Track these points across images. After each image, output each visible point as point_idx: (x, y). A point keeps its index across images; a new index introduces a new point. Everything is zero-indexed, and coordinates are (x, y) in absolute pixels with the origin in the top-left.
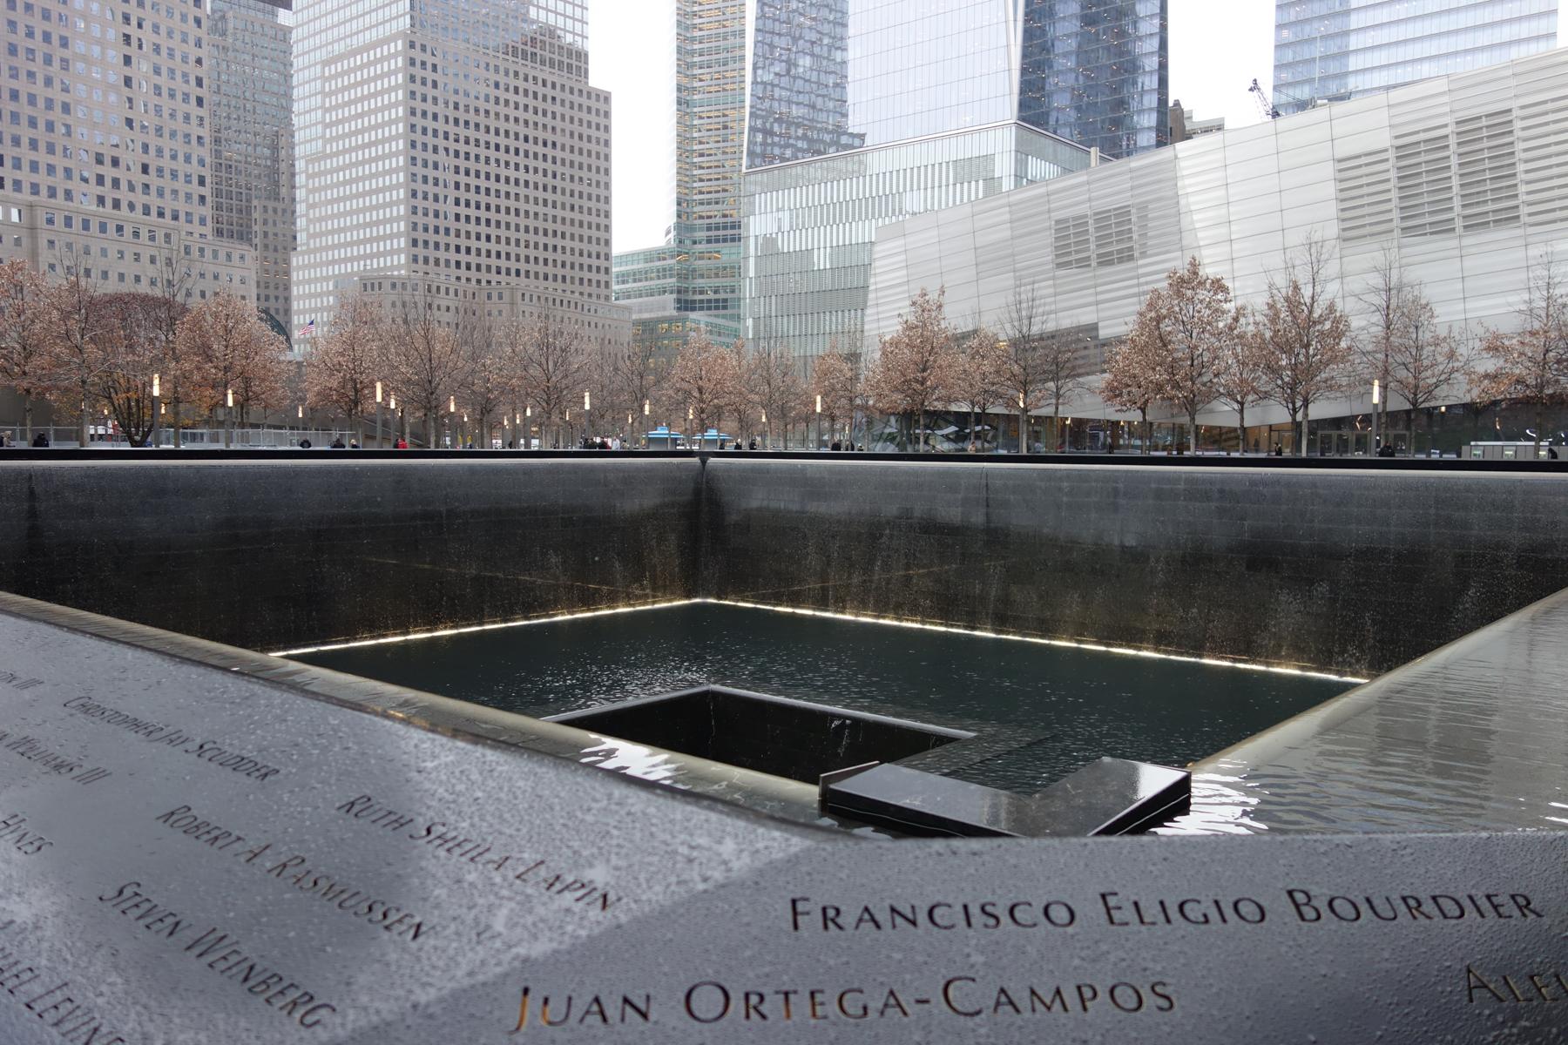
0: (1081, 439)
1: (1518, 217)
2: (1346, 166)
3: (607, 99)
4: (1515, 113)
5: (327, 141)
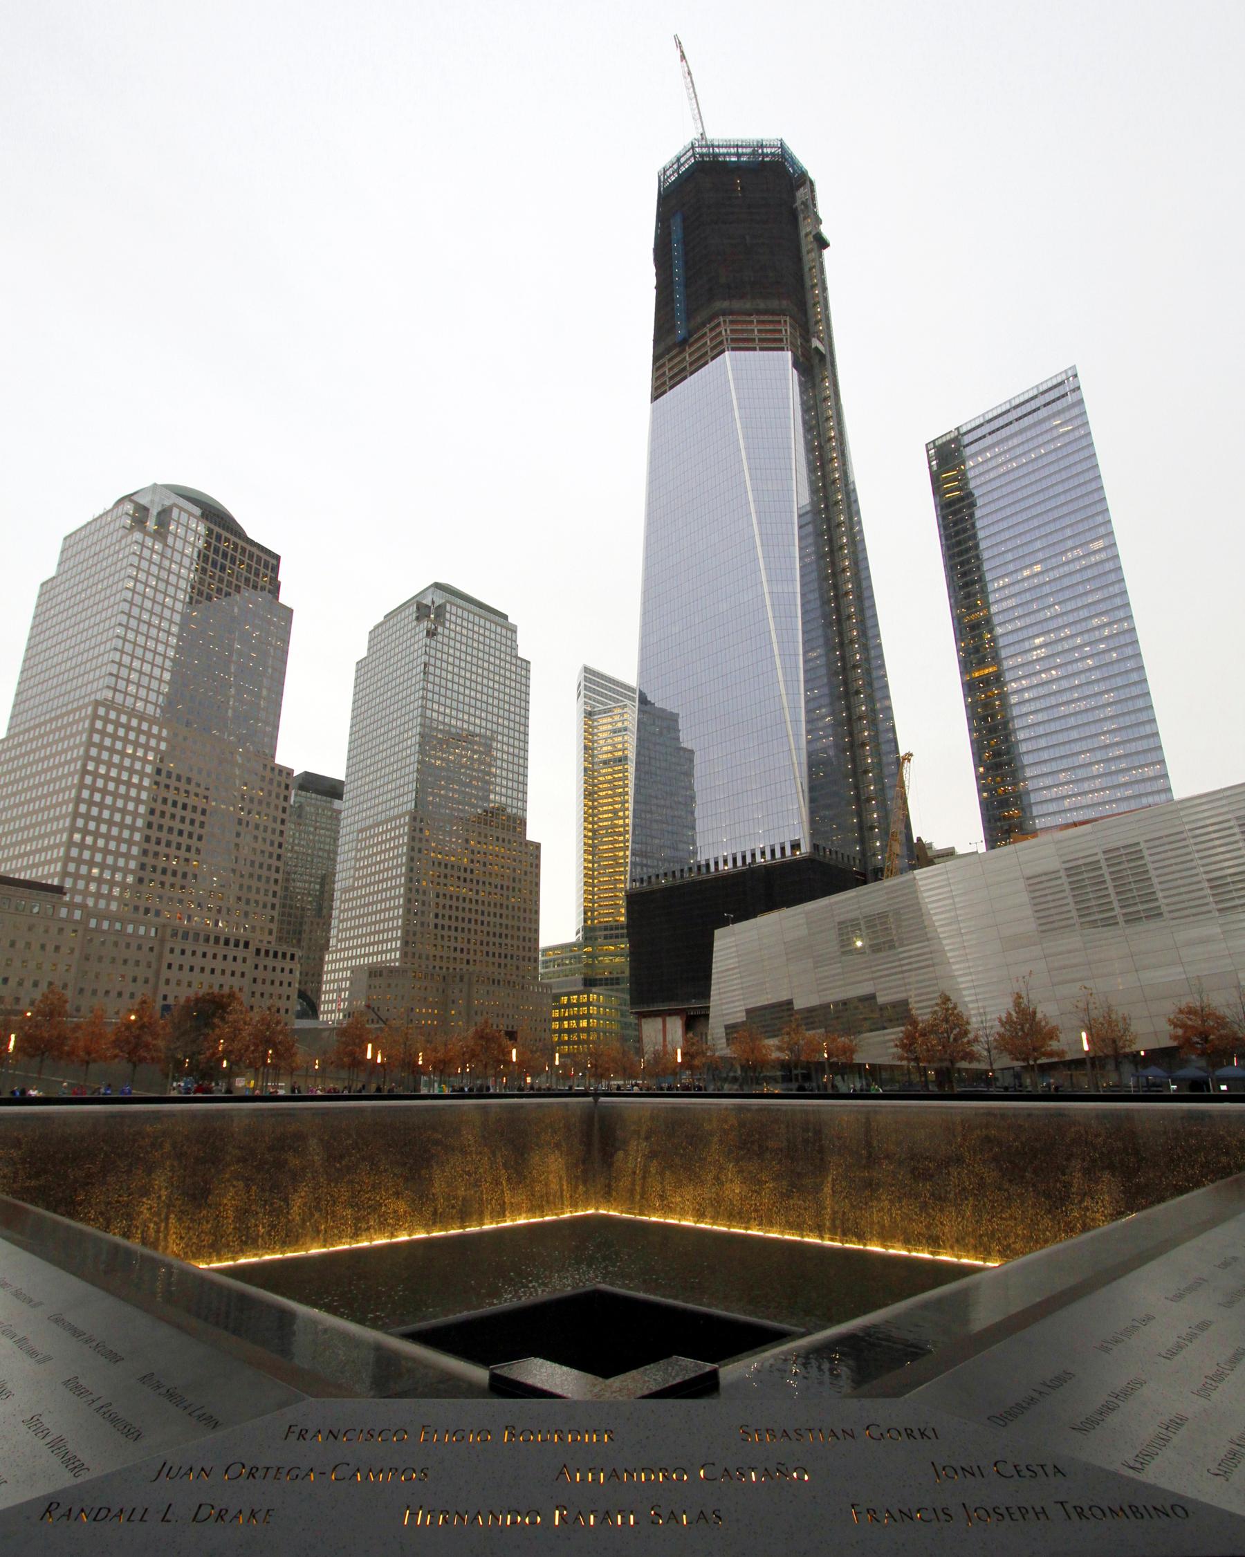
1: (1161, 914)
3: (537, 846)
4: (1143, 845)
5: (356, 879)
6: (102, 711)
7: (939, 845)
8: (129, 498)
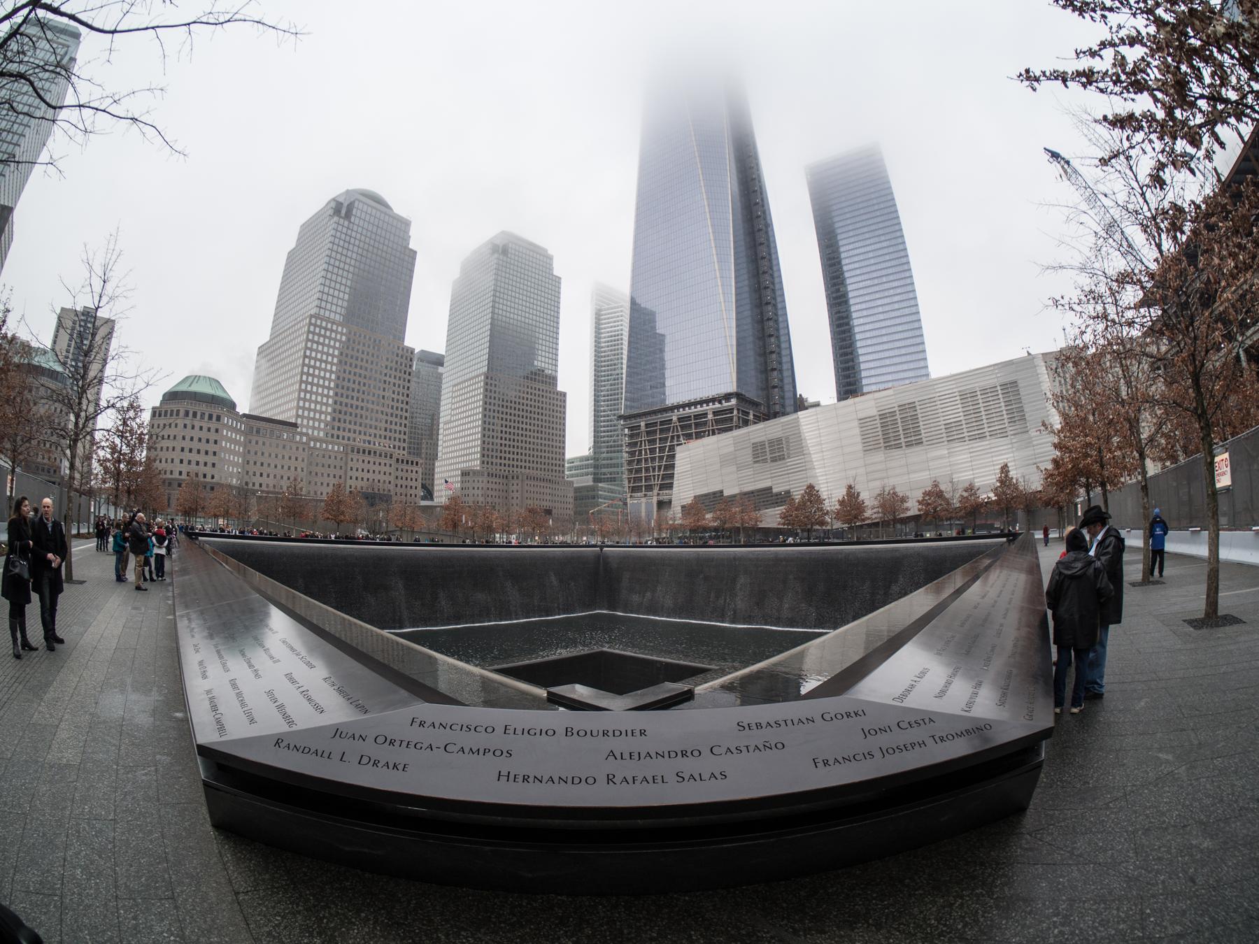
0: (769, 536)
2: (863, 422)
3: (565, 394)
6: (313, 321)
7: (811, 400)
8: (334, 199)
